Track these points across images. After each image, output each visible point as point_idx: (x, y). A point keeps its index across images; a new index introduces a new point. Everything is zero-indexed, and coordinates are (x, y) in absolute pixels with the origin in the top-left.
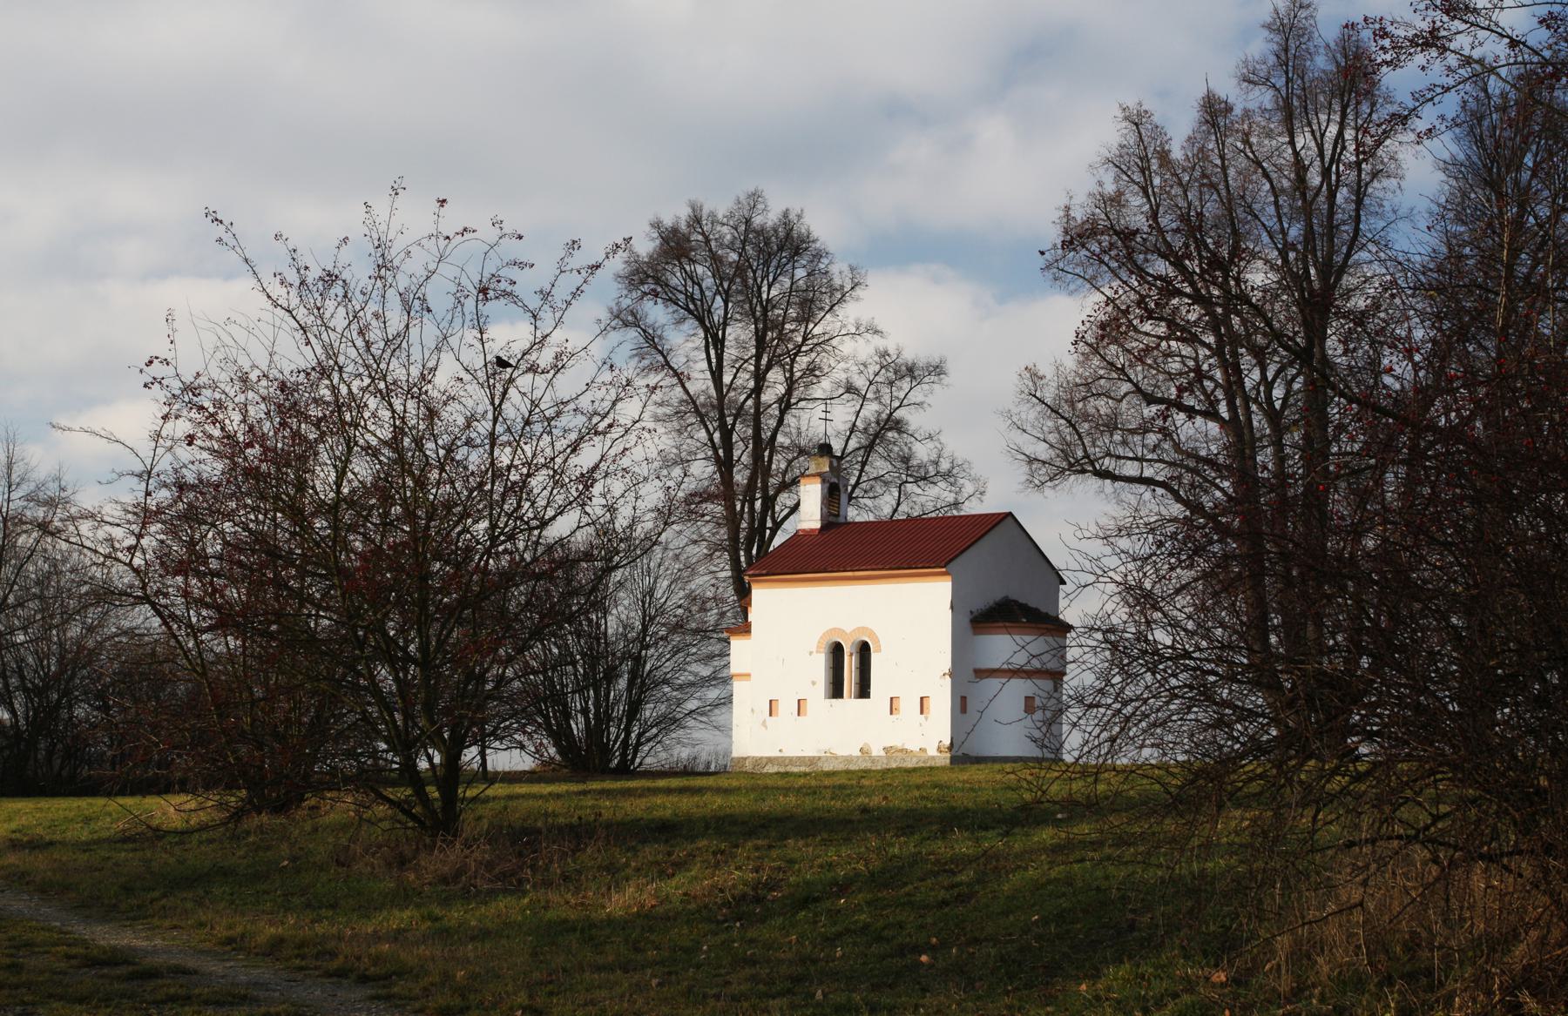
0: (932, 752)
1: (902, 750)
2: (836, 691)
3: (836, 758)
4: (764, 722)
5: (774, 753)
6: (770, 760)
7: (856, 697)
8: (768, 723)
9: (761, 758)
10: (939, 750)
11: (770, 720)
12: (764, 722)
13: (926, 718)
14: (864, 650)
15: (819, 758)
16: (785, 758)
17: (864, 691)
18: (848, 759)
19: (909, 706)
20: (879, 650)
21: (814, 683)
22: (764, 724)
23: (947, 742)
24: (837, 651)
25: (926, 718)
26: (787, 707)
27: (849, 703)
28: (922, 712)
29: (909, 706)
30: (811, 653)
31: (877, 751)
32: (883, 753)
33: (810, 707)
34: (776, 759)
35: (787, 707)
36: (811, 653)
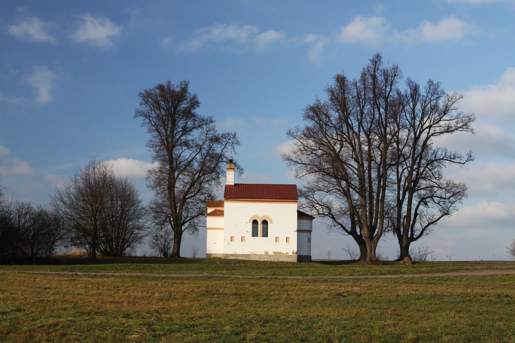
0: (290, 253)
1: (279, 253)
3: (256, 255)
4: (229, 243)
5: (233, 253)
6: (232, 255)
7: (263, 237)
9: (228, 254)
10: (293, 253)
12: (229, 243)
13: (288, 244)
14: (265, 222)
15: (250, 255)
16: (237, 255)
18: (261, 256)
19: (282, 240)
20: (271, 223)
21: (248, 232)
22: (229, 244)
23: (296, 251)
24: (255, 222)
25: (288, 244)
26: (238, 239)
27: (260, 239)
28: (287, 242)
29: (282, 240)
30: (247, 223)
31: (271, 253)
32: (273, 254)
33: (246, 239)
34: (234, 254)
35: (238, 239)
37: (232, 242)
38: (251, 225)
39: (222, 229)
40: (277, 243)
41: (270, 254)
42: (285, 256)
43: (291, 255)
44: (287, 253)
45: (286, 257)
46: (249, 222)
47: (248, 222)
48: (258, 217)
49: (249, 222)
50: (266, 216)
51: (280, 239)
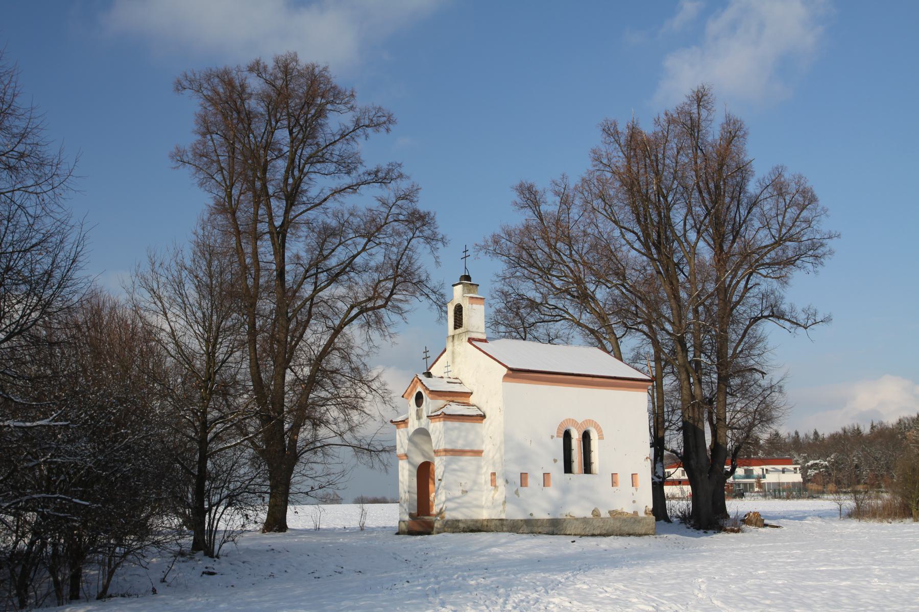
2: (568, 468)
3: (577, 519)
8: (519, 492)
10: (646, 513)
13: (636, 489)
14: (586, 436)
15: (565, 519)
17: (587, 468)
19: (624, 480)
21: (555, 461)
23: (651, 506)
24: (567, 436)
25: (636, 489)
27: (578, 477)
32: (608, 515)
36: (552, 437)
37: (524, 488)
38: (561, 441)
39: (478, 453)
40: (615, 488)
41: (602, 516)
42: (632, 520)
43: (645, 518)
44: (635, 513)
46: (557, 436)
47: (555, 435)
48: (574, 422)
50: (589, 420)
51: (620, 478)
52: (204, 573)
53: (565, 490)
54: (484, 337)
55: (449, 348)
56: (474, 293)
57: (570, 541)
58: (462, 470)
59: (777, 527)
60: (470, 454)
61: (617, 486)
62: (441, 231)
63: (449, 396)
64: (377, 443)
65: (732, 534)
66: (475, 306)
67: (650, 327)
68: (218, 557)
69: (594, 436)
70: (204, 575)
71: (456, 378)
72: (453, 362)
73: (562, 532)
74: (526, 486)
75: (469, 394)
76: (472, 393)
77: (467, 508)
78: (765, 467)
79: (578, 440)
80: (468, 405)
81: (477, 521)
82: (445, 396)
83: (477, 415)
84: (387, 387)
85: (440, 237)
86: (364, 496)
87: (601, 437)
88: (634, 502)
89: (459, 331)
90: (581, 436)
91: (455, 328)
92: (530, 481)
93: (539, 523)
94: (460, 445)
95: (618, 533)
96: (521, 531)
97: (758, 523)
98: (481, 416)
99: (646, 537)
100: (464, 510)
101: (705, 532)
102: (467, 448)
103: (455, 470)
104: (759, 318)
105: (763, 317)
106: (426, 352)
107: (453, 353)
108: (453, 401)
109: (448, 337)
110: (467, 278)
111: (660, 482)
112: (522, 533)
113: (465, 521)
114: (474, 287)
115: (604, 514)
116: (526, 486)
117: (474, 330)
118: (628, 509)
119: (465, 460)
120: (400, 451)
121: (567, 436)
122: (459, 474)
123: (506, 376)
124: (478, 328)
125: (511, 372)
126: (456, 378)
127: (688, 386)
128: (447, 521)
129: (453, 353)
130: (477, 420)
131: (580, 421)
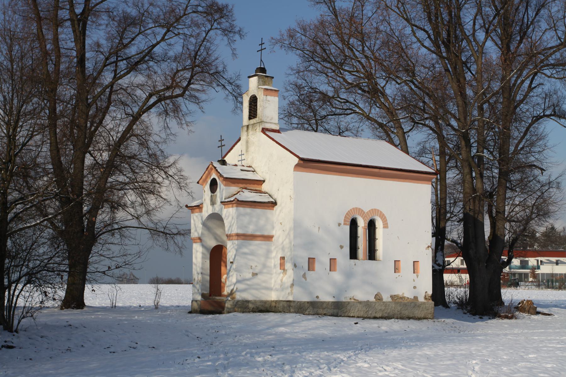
2: (353, 255)
3: (360, 303)
8: (306, 275)
10: (425, 298)
11: (310, 274)
13: (417, 276)
14: (371, 225)
15: (349, 302)
17: (372, 255)
21: (342, 247)
23: (430, 292)
24: (354, 224)
25: (417, 276)
27: (362, 263)
28: (414, 273)
36: (339, 225)
37: (311, 272)
38: (347, 228)
39: (269, 238)
40: (397, 274)
41: (384, 300)
42: (413, 305)
43: (424, 303)
44: (416, 298)
45: (414, 307)
46: (345, 224)
47: (342, 222)
48: (361, 212)
49: (345, 224)
50: (375, 210)
51: (402, 265)
52: (3, 346)
53: (349, 275)
54: (277, 128)
55: (244, 138)
56: (269, 85)
57: (353, 323)
58: (252, 253)
59: (549, 315)
60: (260, 238)
61: (399, 272)
62: (238, 24)
63: (242, 183)
64: (172, 226)
65: (506, 321)
66: (269, 98)
67: (437, 123)
68: (16, 331)
69: (379, 224)
70: (4, 349)
71: (250, 167)
72: (247, 151)
73: (346, 315)
74: (313, 270)
75: (261, 182)
76: (264, 181)
77: (257, 289)
78: (540, 259)
79: (364, 228)
80: (260, 192)
81: (266, 302)
82: (238, 183)
83: (269, 202)
84: (183, 173)
85: (237, 29)
86: (160, 276)
87: (386, 226)
88: (415, 287)
89: (253, 121)
90: (367, 225)
91: (250, 119)
92: (317, 266)
93: (325, 306)
94: (251, 230)
95: (399, 316)
96: (307, 312)
97: (531, 311)
98: (272, 203)
99: (425, 321)
100: (253, 292)
101: (481, 318)
102: (258, 233)
103: (245, 254)
104: (541, 117)
105: (545, 116)
106: (221, 140)
107: (247, 142)
108: (246, 188)
109: (243, 127)
110: (263, 70)
111: (440, 270)
112: (309, 314)
113: (254, 302)
114: (269, 79)
115: (386, 298)
116: (313, 270)
117: (268, 120)
118: (409, 294)
119: (255, 244)
120: (194, 234)
121: (354, 224)
122: (250, 257)
123: (297, 166)
124: (271, 119)
125: (302, 162)
126: (250, 167)
127: (470, 180)
128: (238, 301)
129: (247, 142)
130: (268, 207)
131: (366, 210)
